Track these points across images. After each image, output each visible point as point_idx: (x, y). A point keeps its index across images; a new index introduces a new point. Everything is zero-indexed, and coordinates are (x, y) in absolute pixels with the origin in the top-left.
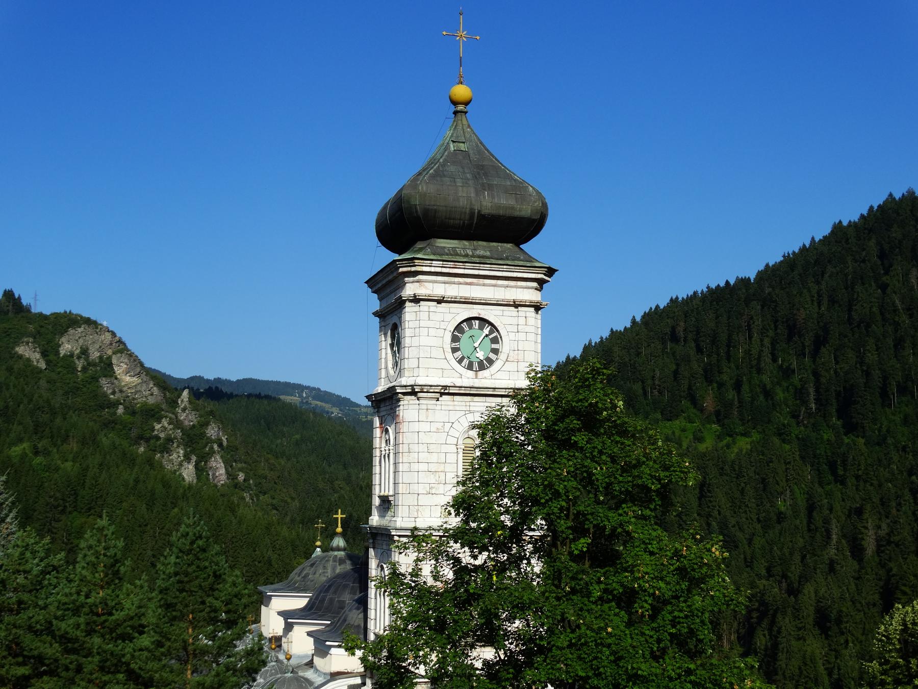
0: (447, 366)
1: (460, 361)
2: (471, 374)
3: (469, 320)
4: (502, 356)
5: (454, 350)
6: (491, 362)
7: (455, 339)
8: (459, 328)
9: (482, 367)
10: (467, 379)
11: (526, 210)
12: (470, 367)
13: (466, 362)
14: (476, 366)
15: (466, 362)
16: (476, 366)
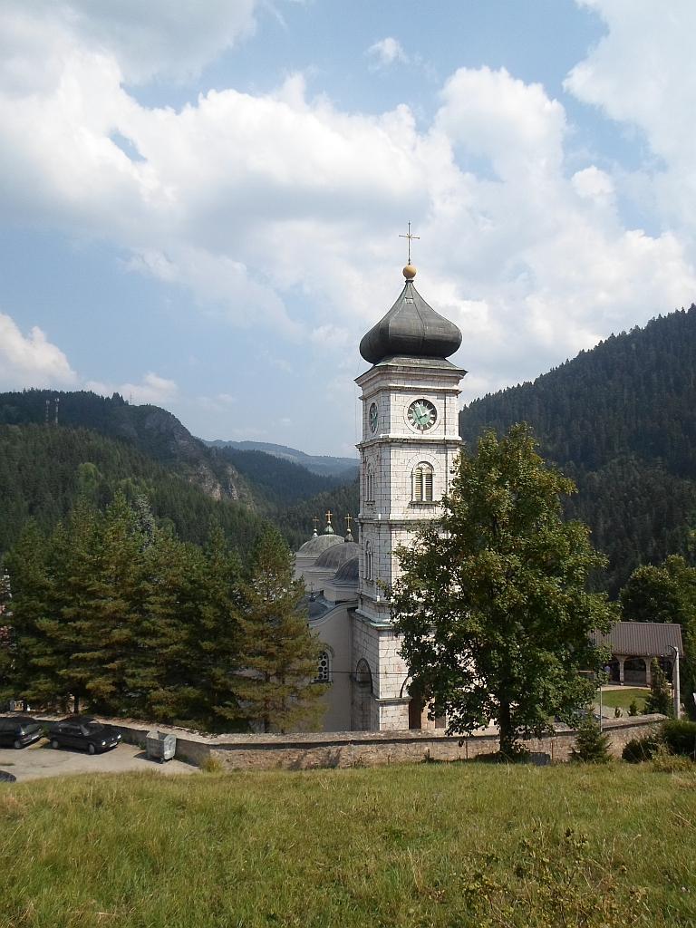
3: (418, 401)
4: (437, 421)
6: (430, 425)
7: (410, 412)
9: (425, 428)
10: (418, 435)
11: (450, 336)
12: (419, 428)
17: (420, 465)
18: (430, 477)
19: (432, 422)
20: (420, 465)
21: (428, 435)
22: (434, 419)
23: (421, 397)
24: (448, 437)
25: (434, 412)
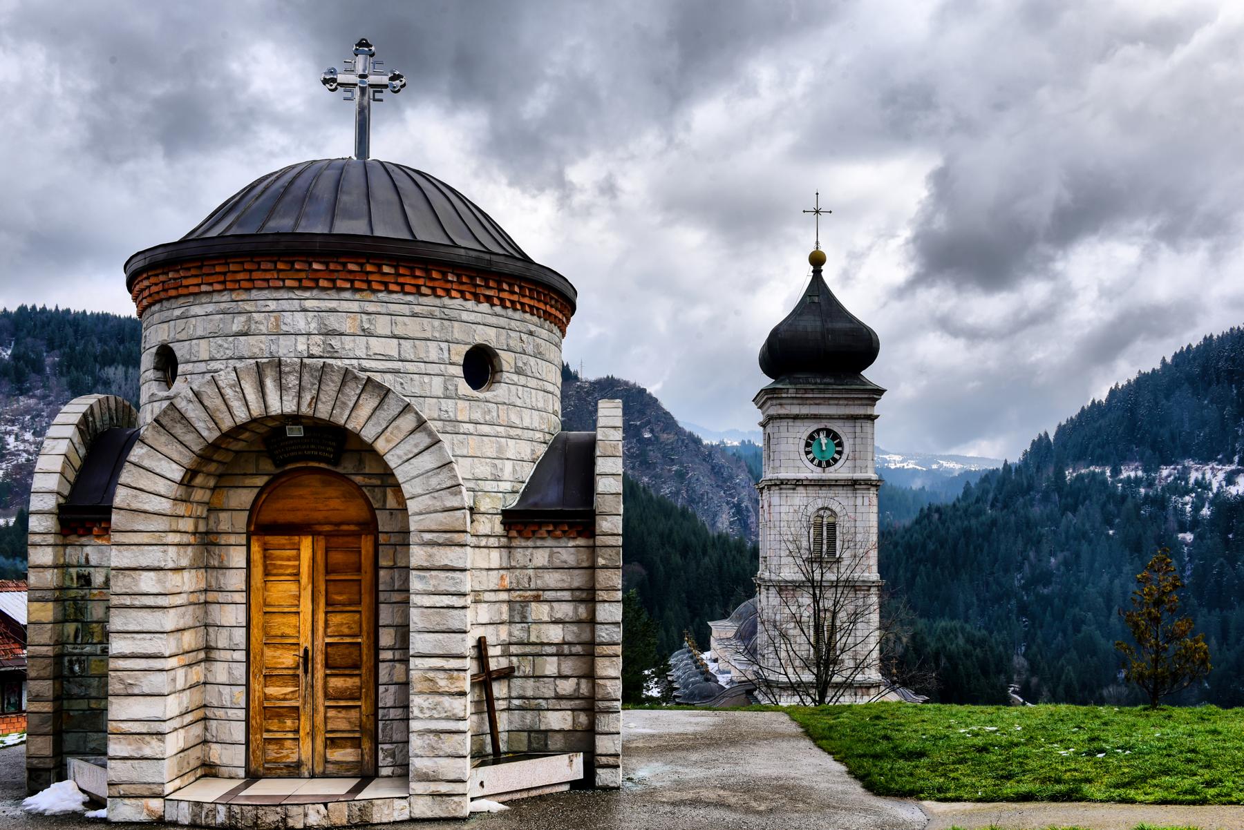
0: (801, 464)
1: (812, 461)
2: (820, 469)
3: (818, 431)
4: (844, 456)
5: (807, 453)
6: (836, 461)
7: (808, 445)
8: (811, 437)
9: (829, 464)
10: (814, 473)
12: (820, 465)
13: (816, 461)
14: (824, 464)
15: (816, 461)
16: (824, 464)
17: (821, 512)
18: (832, 527)
19: (837, 456)
20: (821, 512)
21: (832, 474)
22: (840, 453)
23: (822, 426)
24: (858, 475)
25: (840, 444)
